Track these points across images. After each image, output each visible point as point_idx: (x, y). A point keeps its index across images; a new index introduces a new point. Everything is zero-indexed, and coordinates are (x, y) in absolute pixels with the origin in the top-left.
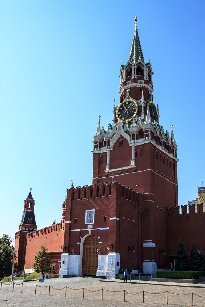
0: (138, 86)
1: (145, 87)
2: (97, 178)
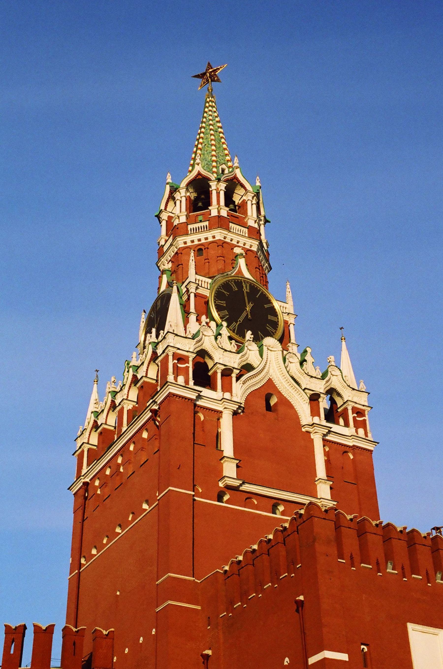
0: (193, 241)
1: (214, 237)
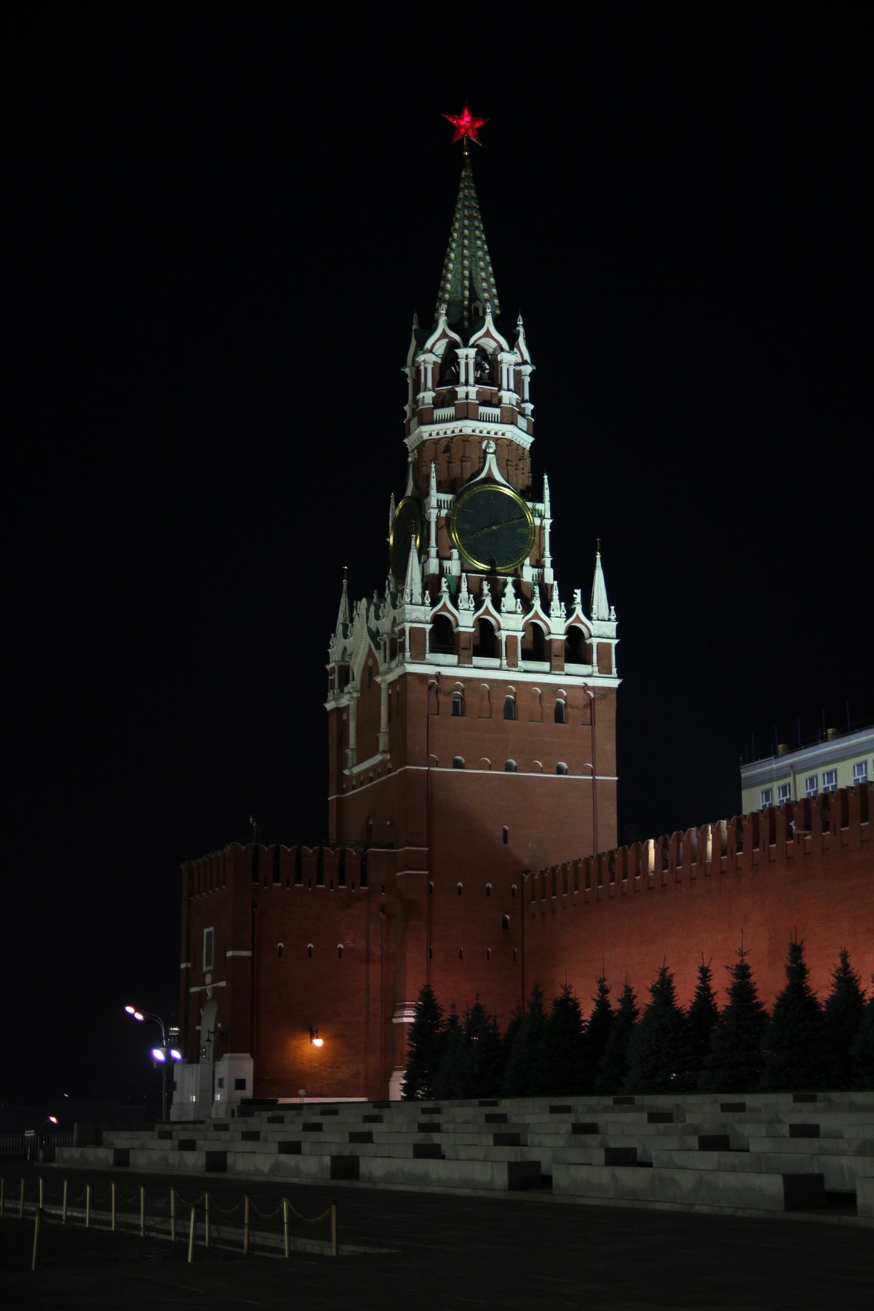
1: (461, 431)
2: (334, 797)
